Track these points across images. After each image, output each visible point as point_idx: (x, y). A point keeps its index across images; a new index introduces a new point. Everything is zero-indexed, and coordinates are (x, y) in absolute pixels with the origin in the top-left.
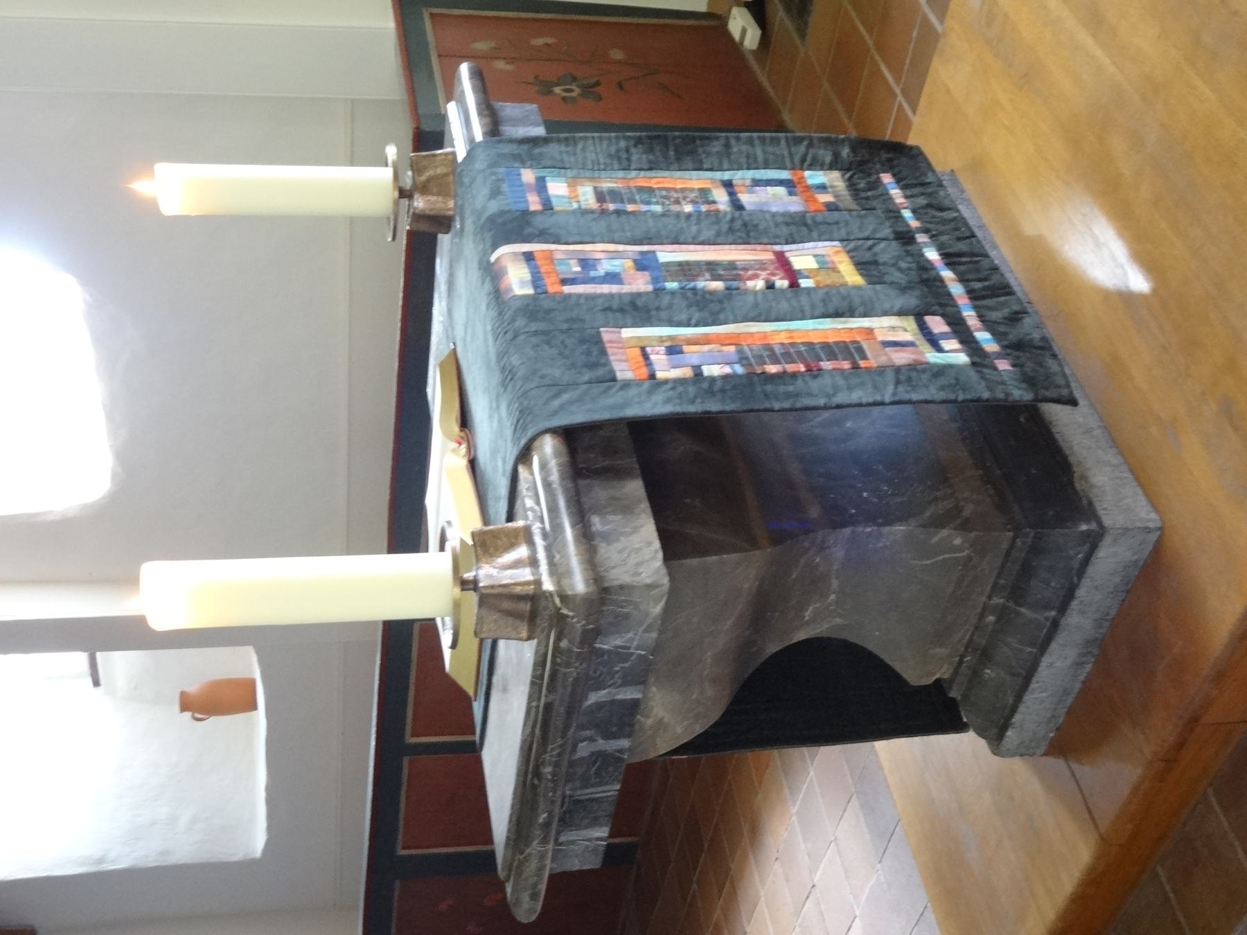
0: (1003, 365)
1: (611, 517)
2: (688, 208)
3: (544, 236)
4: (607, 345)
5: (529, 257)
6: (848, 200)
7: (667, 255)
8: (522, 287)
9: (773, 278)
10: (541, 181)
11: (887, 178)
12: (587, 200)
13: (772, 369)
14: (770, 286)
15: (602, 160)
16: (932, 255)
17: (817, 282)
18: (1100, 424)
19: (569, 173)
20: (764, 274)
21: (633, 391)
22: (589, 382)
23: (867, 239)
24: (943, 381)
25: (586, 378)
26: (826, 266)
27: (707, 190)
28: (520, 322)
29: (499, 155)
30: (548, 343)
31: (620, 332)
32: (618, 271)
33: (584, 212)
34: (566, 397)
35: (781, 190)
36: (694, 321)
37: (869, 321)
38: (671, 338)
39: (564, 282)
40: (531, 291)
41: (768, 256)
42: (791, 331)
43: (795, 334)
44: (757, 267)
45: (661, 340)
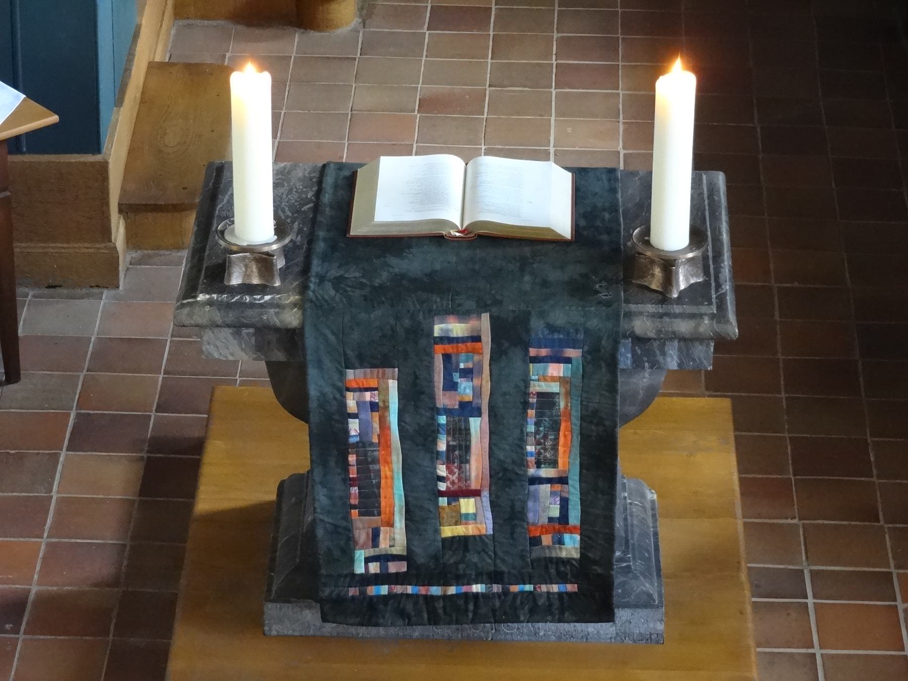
0: (353, 592)
1: (253, 340)
2: (530, 448)
4: (381, 370)
5: (476, 339)
6: (536, 553)
7: (478, 426)
9: (448, 482)
10: (568, 360)
11: (571, 588)
12: (534, 386)
13: (352, 459)
14: (442, 479)
15: (591, 404)
16: (477, 588)
17: (443, 508)
18: (361, 635)
19: (578, 381)
20: (454, 478)
21: (336, 377)
22: (345, 354)
23: (495, 553)
24: (337, 553)
25: (349, 352)
26: (460, 519)
27: (555, 464)
28: (407, 322)
29: (600, 339)
30: (384, 336)
31: (393, 379)
32: (459, 390)
33: (526, 382)
34: (332, 338)
35: (555, 512)
36: (403, 424)
37: (401, 528)
38: (386, 408)
39: (447, 357)
40: (436, 334)
41: (474, 485)
42: (392, 478)
43: (389, 480)
44: (463, 475)
45: (386, 402)
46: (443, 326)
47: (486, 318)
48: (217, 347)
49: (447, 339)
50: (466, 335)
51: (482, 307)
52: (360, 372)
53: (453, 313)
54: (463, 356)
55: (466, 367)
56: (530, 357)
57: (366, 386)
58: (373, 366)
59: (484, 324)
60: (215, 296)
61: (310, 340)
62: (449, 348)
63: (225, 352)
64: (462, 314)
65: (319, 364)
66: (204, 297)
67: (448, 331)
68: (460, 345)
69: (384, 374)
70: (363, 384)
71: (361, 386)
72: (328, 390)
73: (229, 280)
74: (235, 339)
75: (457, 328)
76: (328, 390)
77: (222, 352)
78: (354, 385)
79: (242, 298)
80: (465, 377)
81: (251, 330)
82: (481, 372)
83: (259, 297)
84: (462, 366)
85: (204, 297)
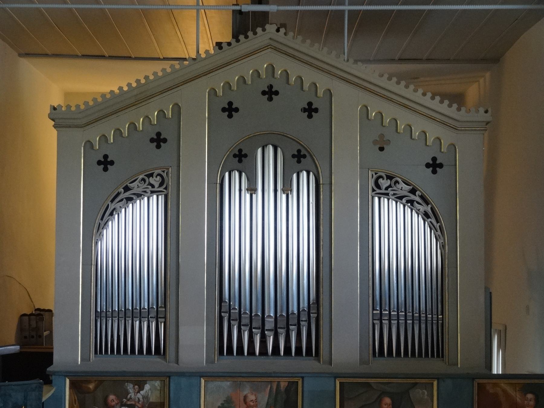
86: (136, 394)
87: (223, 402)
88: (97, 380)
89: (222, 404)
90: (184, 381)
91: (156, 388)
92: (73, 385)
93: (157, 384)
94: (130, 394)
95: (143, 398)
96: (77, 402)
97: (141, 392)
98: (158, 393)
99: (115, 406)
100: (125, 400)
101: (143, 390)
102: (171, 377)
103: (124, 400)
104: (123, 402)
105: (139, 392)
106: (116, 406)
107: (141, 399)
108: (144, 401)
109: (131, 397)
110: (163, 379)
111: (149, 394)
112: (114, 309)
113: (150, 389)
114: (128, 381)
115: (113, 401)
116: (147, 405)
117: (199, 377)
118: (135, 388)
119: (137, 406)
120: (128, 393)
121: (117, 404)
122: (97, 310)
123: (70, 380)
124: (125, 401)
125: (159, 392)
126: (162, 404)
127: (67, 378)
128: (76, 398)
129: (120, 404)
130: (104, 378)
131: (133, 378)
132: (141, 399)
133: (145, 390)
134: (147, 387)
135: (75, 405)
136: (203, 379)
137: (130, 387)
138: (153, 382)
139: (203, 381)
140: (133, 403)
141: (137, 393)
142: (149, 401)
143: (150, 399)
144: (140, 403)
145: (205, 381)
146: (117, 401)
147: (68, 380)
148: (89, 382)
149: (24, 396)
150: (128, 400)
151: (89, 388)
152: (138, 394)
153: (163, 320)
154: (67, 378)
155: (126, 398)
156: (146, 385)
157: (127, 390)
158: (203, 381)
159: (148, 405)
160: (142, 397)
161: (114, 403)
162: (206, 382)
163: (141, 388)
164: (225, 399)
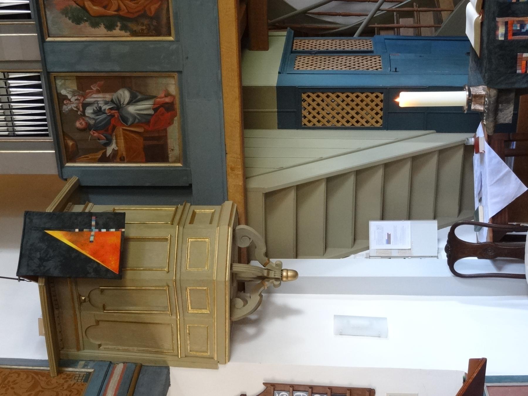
1: (504, 104)
3: (514, 14)
4: (518, 60)
8: (501, 37)
21: (519, 77)
25: (509, 72)
31: (523, 55)
34: (502, 78)
39: (514, 34)
46: (499, 36)
47: (498, 19)
48: (506, 118)
49: (506, 35)
50: (504, 27)
51: (494, 19)
52: (518, 68)
53: (495, 32)
54: (514, 28)
55: (519, 27)
56: (516, 1)
57: (525, 65)
58: (516, 63)
59: (500, 20)
60: (484, 118)
61: (503, 87)
62: (510, 34)
63: (509, 115)
64: (496, 28)
65: (514, 83)
66: (485, 122)
67: (502, 35)
68: (509, 29)
69: (519, 58)
70: (524, 66)
71: (525, 67)
72: (525, 80)
73: (482, 110)
74: (503, 111)
75: (501, 31)
76: (525, 80)
77: (509, 116)
78: (524, 70)
79: (486, 108)
80: (524, 27)
81: (500, 105)
82: (523, 21)
83: (486, 102)
84: (519, 28)
85: (485, 122)
86: (72, 103)
87: (68, 17)
88: (64, 138)
89: (70, 18)
90: (50, 58)
91: (64, 84)
92: (72, 159)
93: (59, 83)
94: (73, 108)
95: (75, 96)
96: (87, 156)
97: (69, 97)
98: (68, 82)
99: (86, 121)
100: (79, 113)
101: (66, 96)
102: (49, 71)
103: (79, 113)
104: (81, 114)
105: (70, 100)
106: (85, 121)
107: (76, 97)
108: (77, 95)
109: (74, 107)
110: (52, 79)
111: (70, 90)
112: (4, 120)
113: (65, 89)
114: (61, 111)
115: (81, 123)
116: (81, 92)
117: (45, 44)
118: (67, 103)
119: (83, 100)
120: (72, 110)
121: (84, 120)
122: (7, 134)
123: (68, 162)
124: (80, 113)
125: (67, 81)
126: (78, 78)
127: (66, 165)
128: (83, 156)
129: (83, 117)
130: (61, 133)
131: (56, 107)
132: (76, 97)
133: (67, 94)
134: (63, 92)
135: (90, 158)
136: (46, 38)
137: (66, 108)
138: (58, 87)
139: (49, 39)
140: (80, 105)
141: (71, 101)
142: (76, 90)
143: (74, 90)
144: (79, 99)
145: (49, 37)
146: (81, 120)
147: (67, 164)
148: (66, 146)
149: (35, 230)
150: (79, 109)
151: (73, 144)
152: (71, 100)
153: (6, 74)
154: (66, 165)
155: (77, 112)
156: (62, 94)
157: (69, 110)
158: (49, 39)
159: (80, 91)
160: (74, 97)
161: (83, 123)
162: (50, 36)
163: (65, 98)
164: (64, 16)
